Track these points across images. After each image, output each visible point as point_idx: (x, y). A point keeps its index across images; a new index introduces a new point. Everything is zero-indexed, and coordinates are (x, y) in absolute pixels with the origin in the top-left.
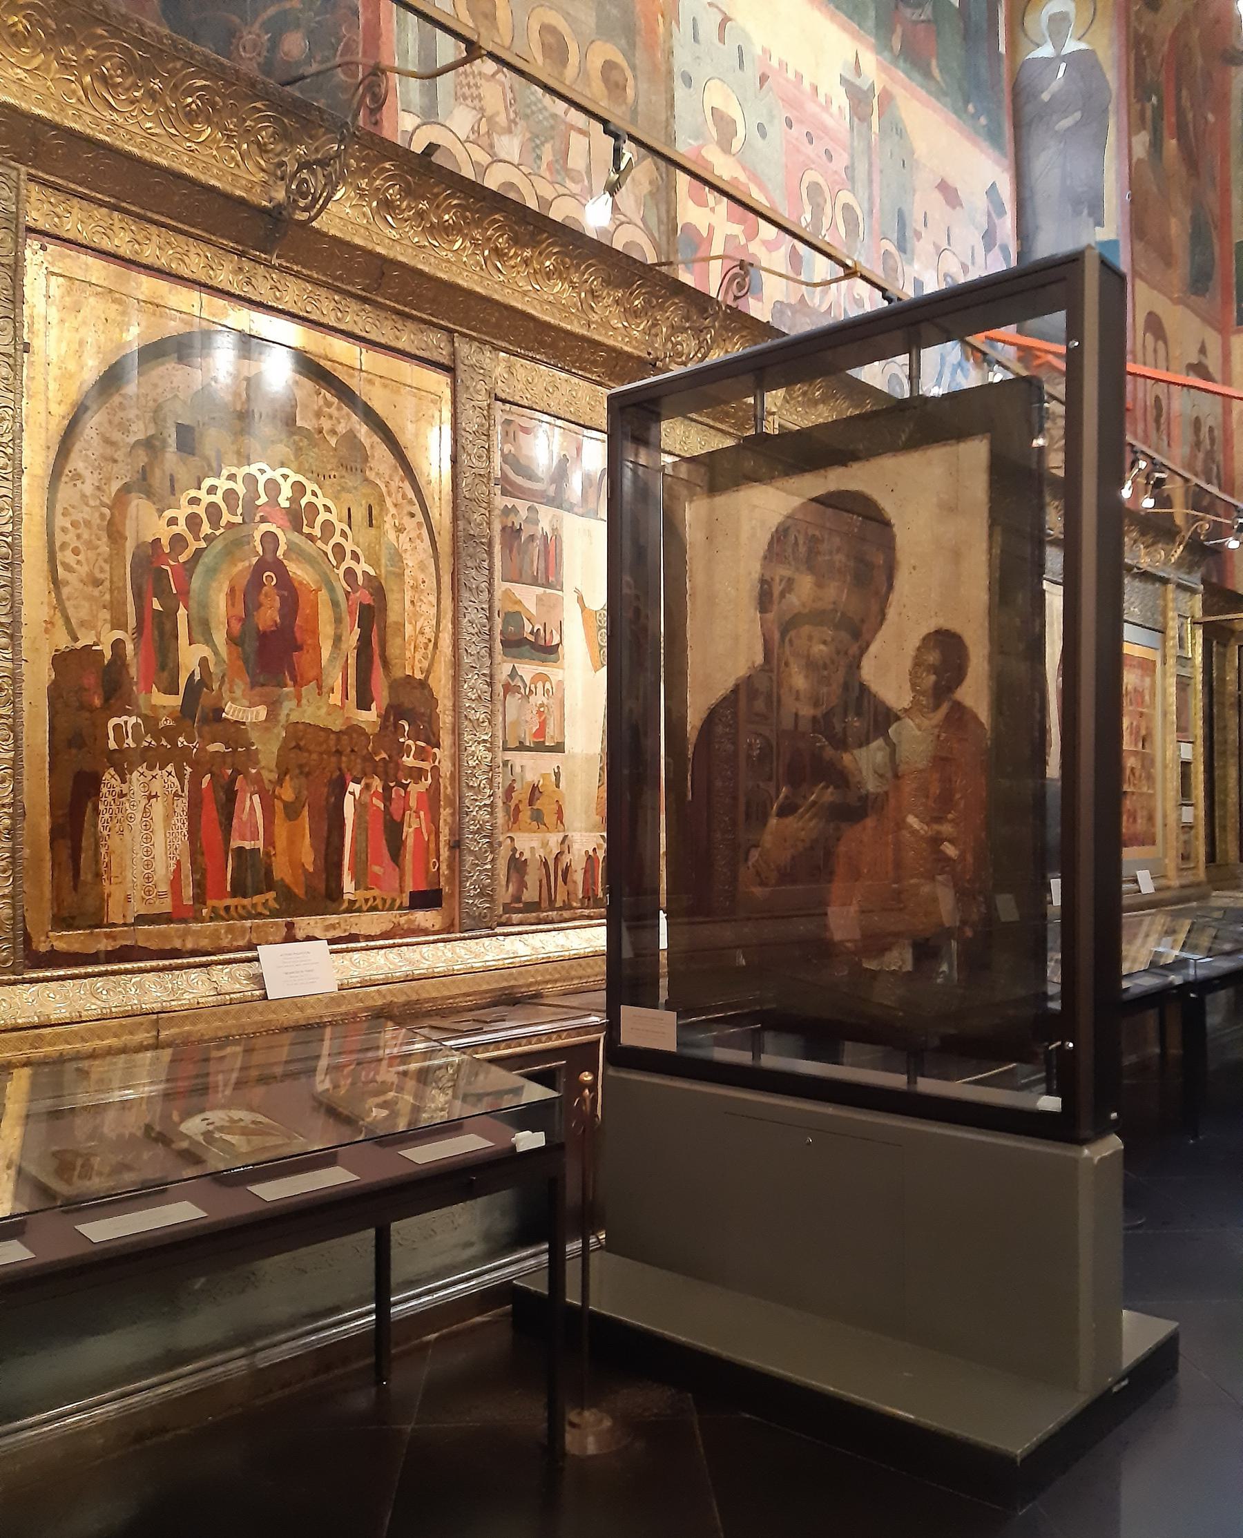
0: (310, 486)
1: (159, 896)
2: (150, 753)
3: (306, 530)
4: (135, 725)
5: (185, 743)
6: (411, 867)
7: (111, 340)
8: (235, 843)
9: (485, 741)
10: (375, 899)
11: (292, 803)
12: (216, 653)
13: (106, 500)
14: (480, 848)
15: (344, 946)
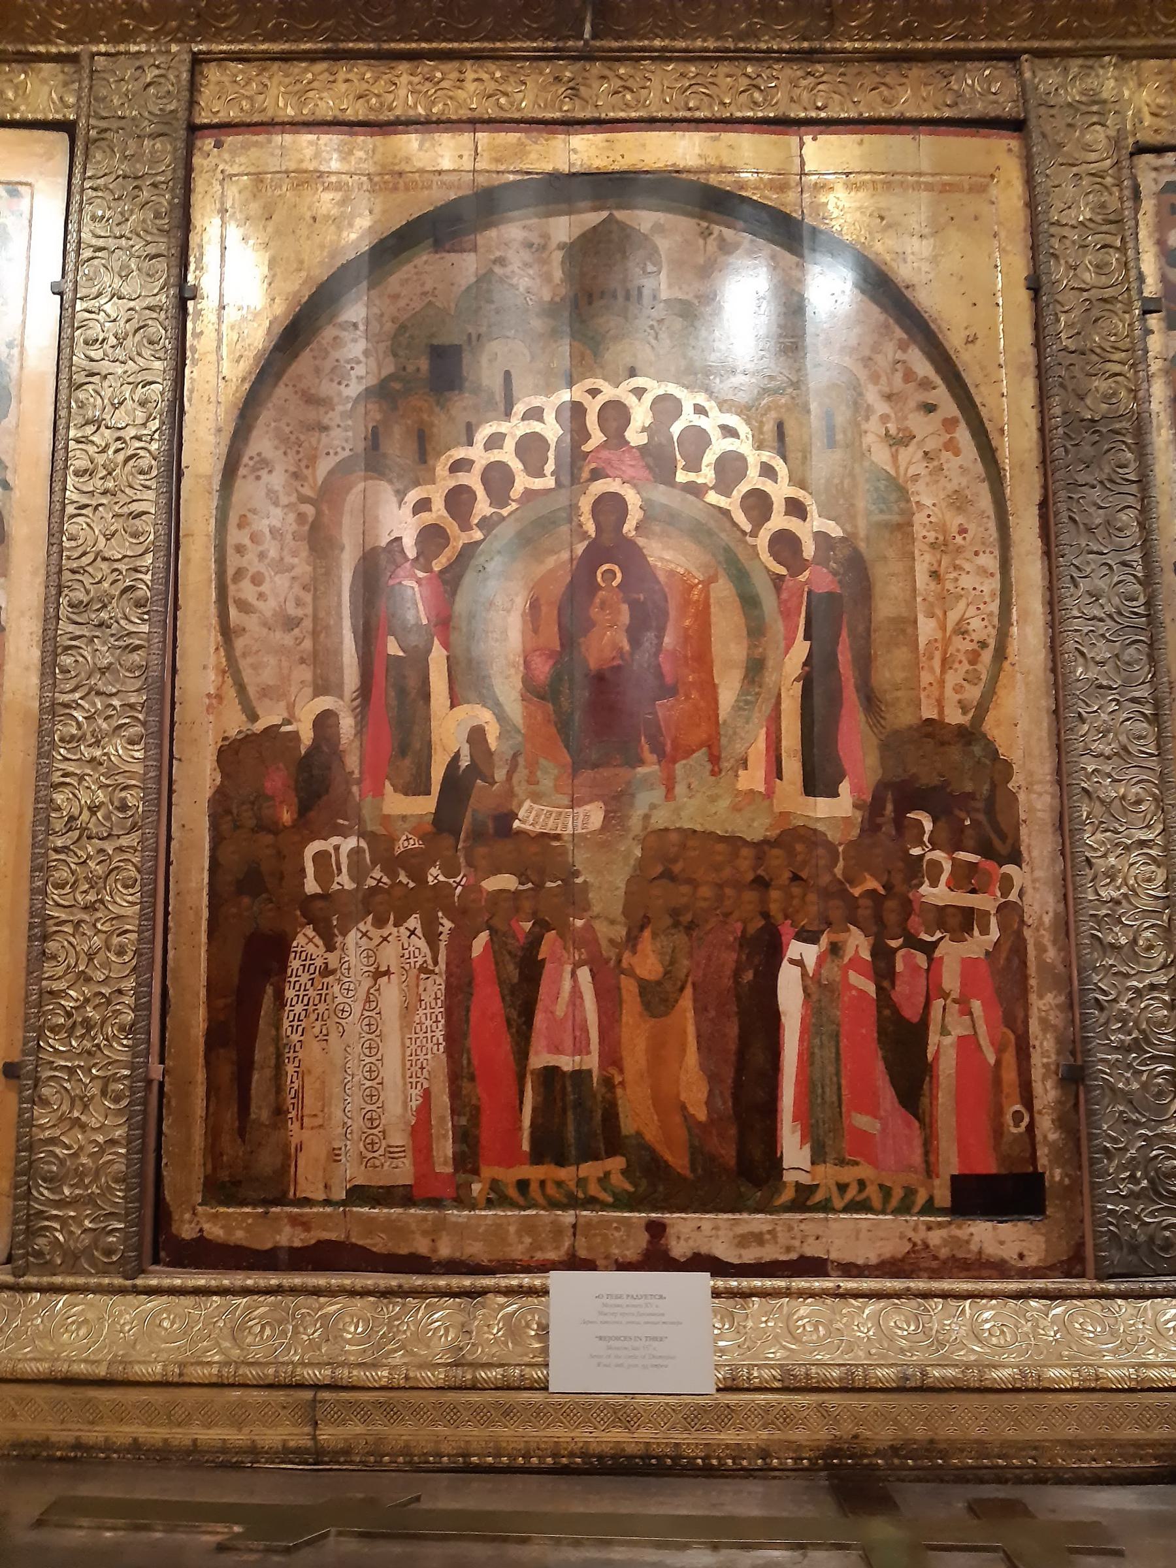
0: (688, 399)
1: (390, 1152)
2: (379, 898)
3: (682, 477)
4: (356, 852)
5: (441, 878)
6: (953, 1121)
7: (322, 247)
8: (539, 1059)
9: (1142, 843)
10: (862, 1184)
11: (659, 983)
12: (501, 717)
13: (307, 491)
14: (1145, 1086)
15: (781, 1283)
